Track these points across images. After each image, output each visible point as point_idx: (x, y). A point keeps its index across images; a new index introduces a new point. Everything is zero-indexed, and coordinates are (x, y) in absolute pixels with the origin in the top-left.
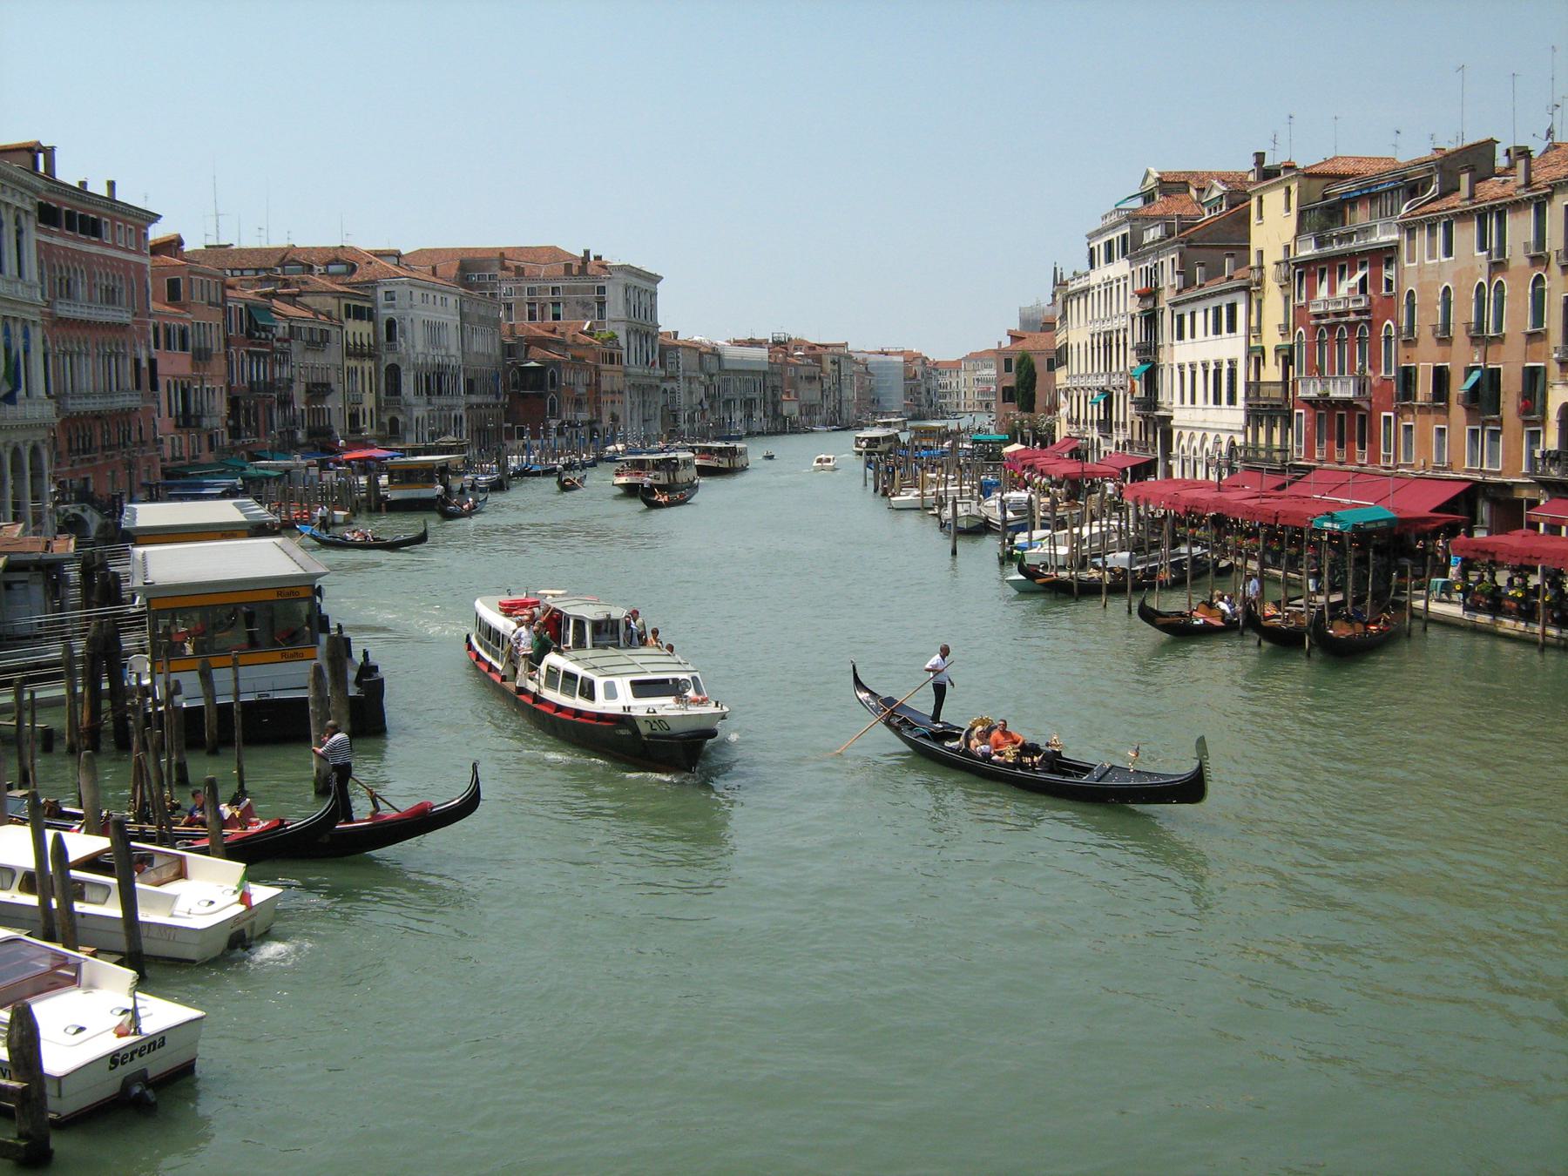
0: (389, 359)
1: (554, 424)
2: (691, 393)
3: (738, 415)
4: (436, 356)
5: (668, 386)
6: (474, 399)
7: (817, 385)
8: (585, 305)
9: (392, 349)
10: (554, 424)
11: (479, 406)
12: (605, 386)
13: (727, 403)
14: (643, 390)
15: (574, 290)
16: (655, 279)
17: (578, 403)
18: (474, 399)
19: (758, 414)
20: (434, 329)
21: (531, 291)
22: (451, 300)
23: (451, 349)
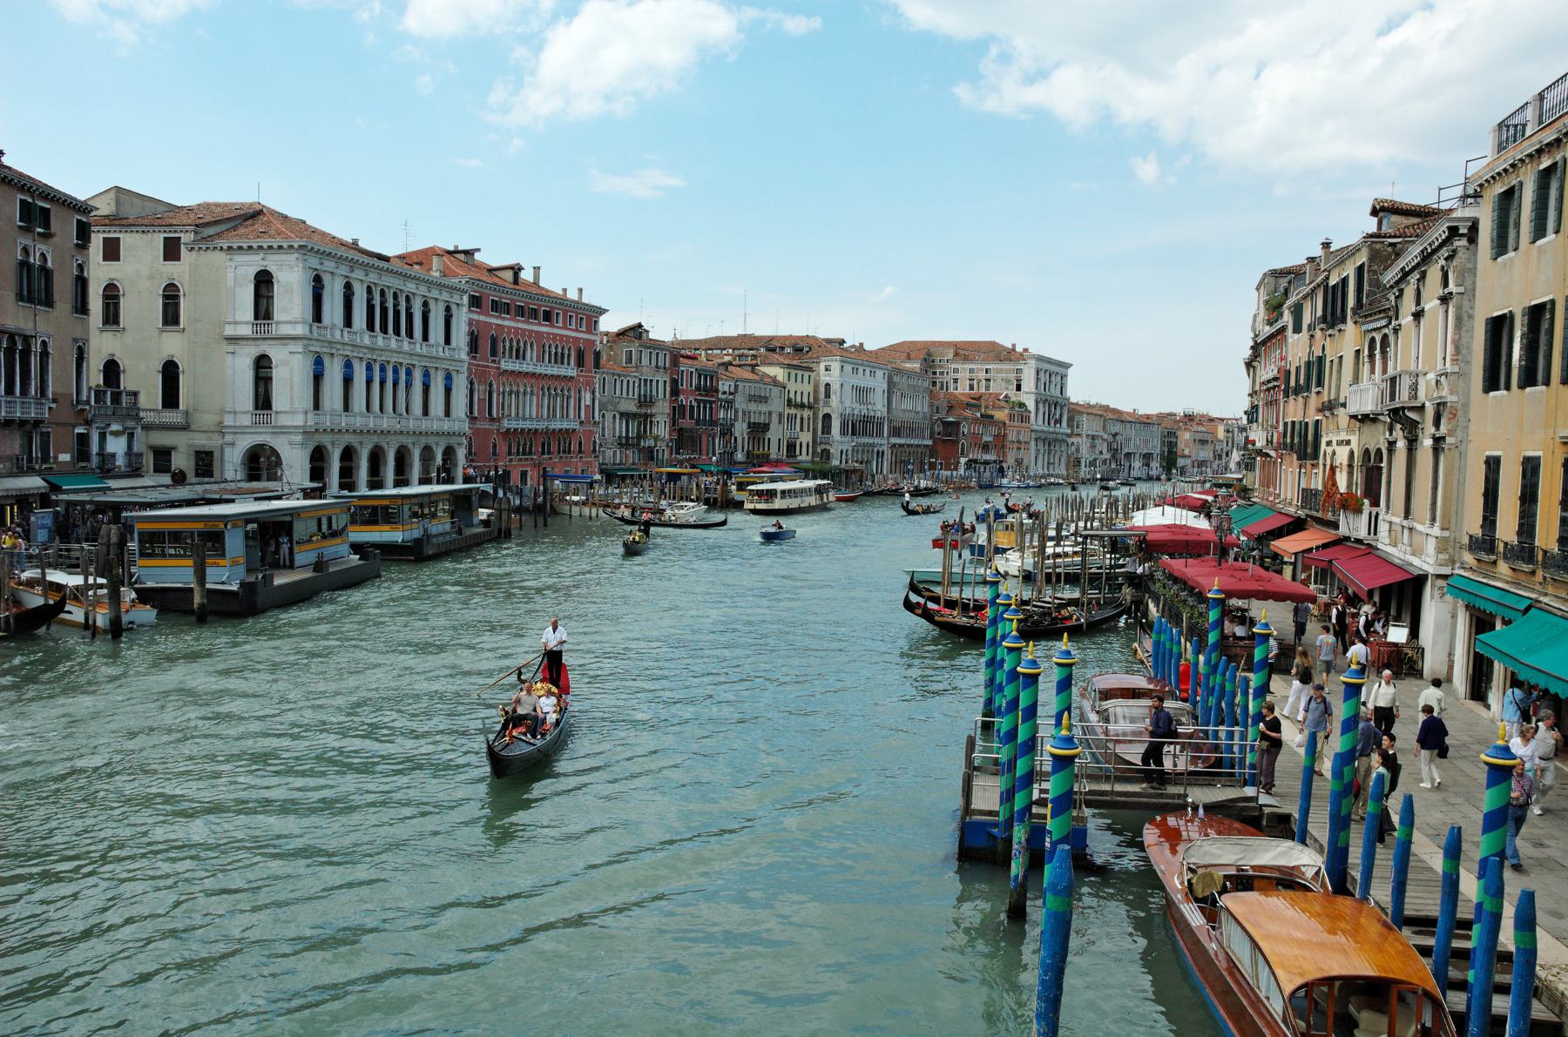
0: (823, 411)
1: (963, 460)
2: (1093, 446)
3: (1137, 464)
4: (859, 410)
5: (1075, 440)
6: (895, 440)
7: (1210, 447)
8: (1008, 381)
9: (827, 404)
10: (963, 460)
11: (901, 445)
12: (1012, 436)
13: (1128, 455)
14: (1050, 442)
15: (1001, 371)
16: (1067, 366)
17: (986, 448)
18: (895, 440)
19: (1155, 464)
20: (862, 393)
21: (971, 371)
22: (879, 373)
23: (879, 407)
